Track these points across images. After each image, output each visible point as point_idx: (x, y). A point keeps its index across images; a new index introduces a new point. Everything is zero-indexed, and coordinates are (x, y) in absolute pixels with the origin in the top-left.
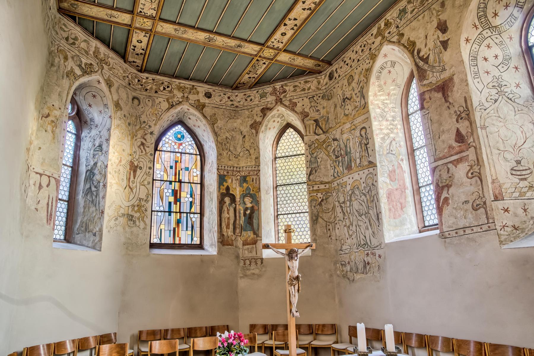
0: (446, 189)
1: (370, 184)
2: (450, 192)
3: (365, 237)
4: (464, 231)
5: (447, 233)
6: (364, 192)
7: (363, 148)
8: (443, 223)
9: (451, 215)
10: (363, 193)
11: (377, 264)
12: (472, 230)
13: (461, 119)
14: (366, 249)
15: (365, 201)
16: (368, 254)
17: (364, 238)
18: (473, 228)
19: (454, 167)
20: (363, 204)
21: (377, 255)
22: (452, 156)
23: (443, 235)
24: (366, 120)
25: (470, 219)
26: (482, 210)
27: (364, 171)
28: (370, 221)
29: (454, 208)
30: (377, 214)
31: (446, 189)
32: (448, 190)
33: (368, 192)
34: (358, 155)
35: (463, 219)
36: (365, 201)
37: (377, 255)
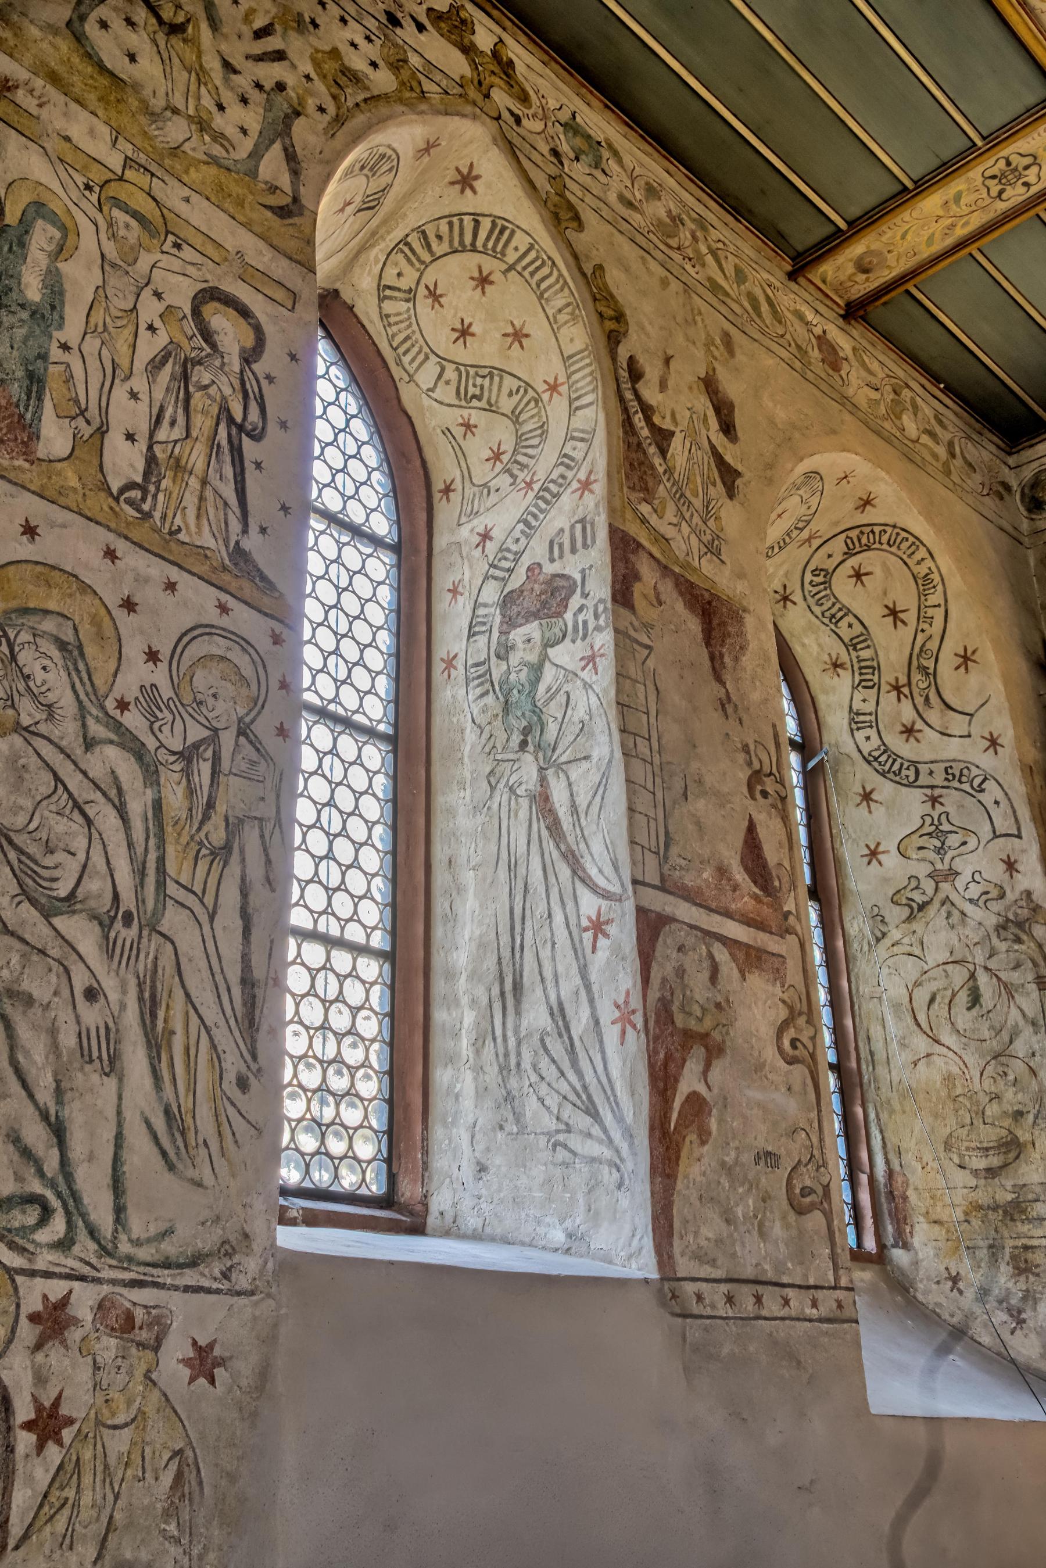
0: (698, 1052)
1: (225, 711)
2: (716, 1074)
3: (59, 1132)
4: (759, 1299)
5: (690, 1288)
6: (133, 720)
7: (202, 424)
8: (677, 1224)
9: (707, 1198)
10: (118, 727)
11: (161, 1437)
12: (786, 1302)
13: (765, 794)
14: (45, 1260)
15: (137, 806)
16: (54, 1321)
17: (36, 1135)
18: (790, 1293)
19: (735, 972)
20: (107, 819)
21: (176, 1349)
22: (727, 914)
23: (674, 1296)
24: (279, 295)
25: (776, 1242)
26: (817, 1217)
27: (175, 574)
28: (150, 1007)
29: (723, 1164)
30: (247, 982)
31: (698, 1052)
32: (708, 1066)
33: (188, 756)
34: (127, 413)
35: (755, 1233)
36: (137, 806)
37: (176, 1349)
